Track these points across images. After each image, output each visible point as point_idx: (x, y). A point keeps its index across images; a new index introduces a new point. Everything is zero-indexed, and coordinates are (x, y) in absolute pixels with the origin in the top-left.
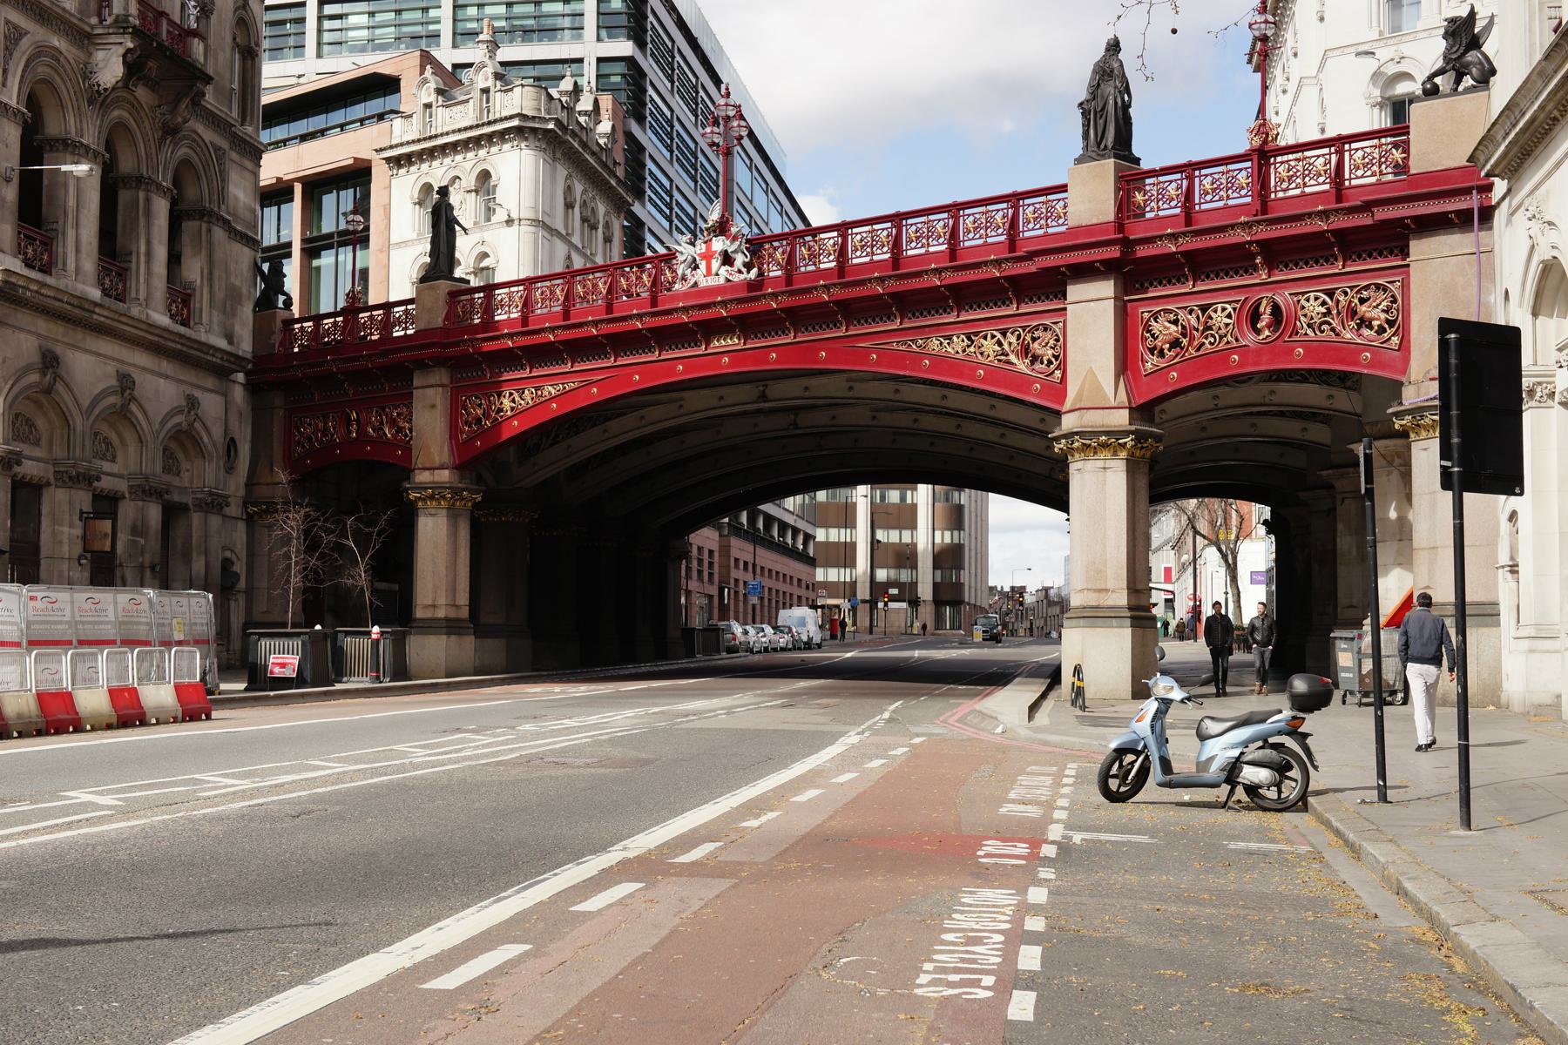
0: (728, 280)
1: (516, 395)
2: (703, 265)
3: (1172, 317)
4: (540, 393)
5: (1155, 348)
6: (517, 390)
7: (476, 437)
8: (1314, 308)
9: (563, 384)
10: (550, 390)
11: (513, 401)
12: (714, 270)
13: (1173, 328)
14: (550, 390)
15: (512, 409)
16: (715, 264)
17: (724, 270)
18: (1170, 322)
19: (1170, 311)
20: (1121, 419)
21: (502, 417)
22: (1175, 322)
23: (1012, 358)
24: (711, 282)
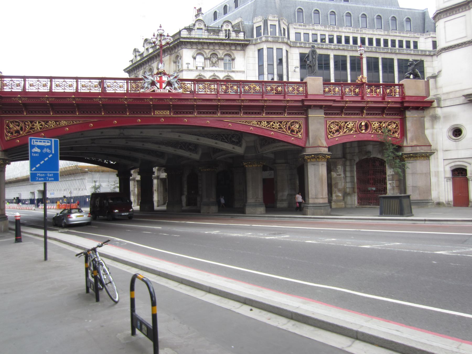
0: (169, 91)
1: (43, 123)
2: (158, 85)
3: (337, 124)
4: (58, 123)
5: (332, 131)
6: (44, 121)
7: (17, 138)
8: (377, 125)
9: (72, 121)
10: (63, 123)
11: (41, 125)
12: (163, 87)
13: (337, 127)
14: (63, 123)
15: (41, 128)
16: (164, 85)
17: (168, 88)
18: (336, 125)
19: (336, 122)
20: (325, 151)
21: (33, 131)
22: (338, 125)
23: (285, 130)
24: (162, 91)
